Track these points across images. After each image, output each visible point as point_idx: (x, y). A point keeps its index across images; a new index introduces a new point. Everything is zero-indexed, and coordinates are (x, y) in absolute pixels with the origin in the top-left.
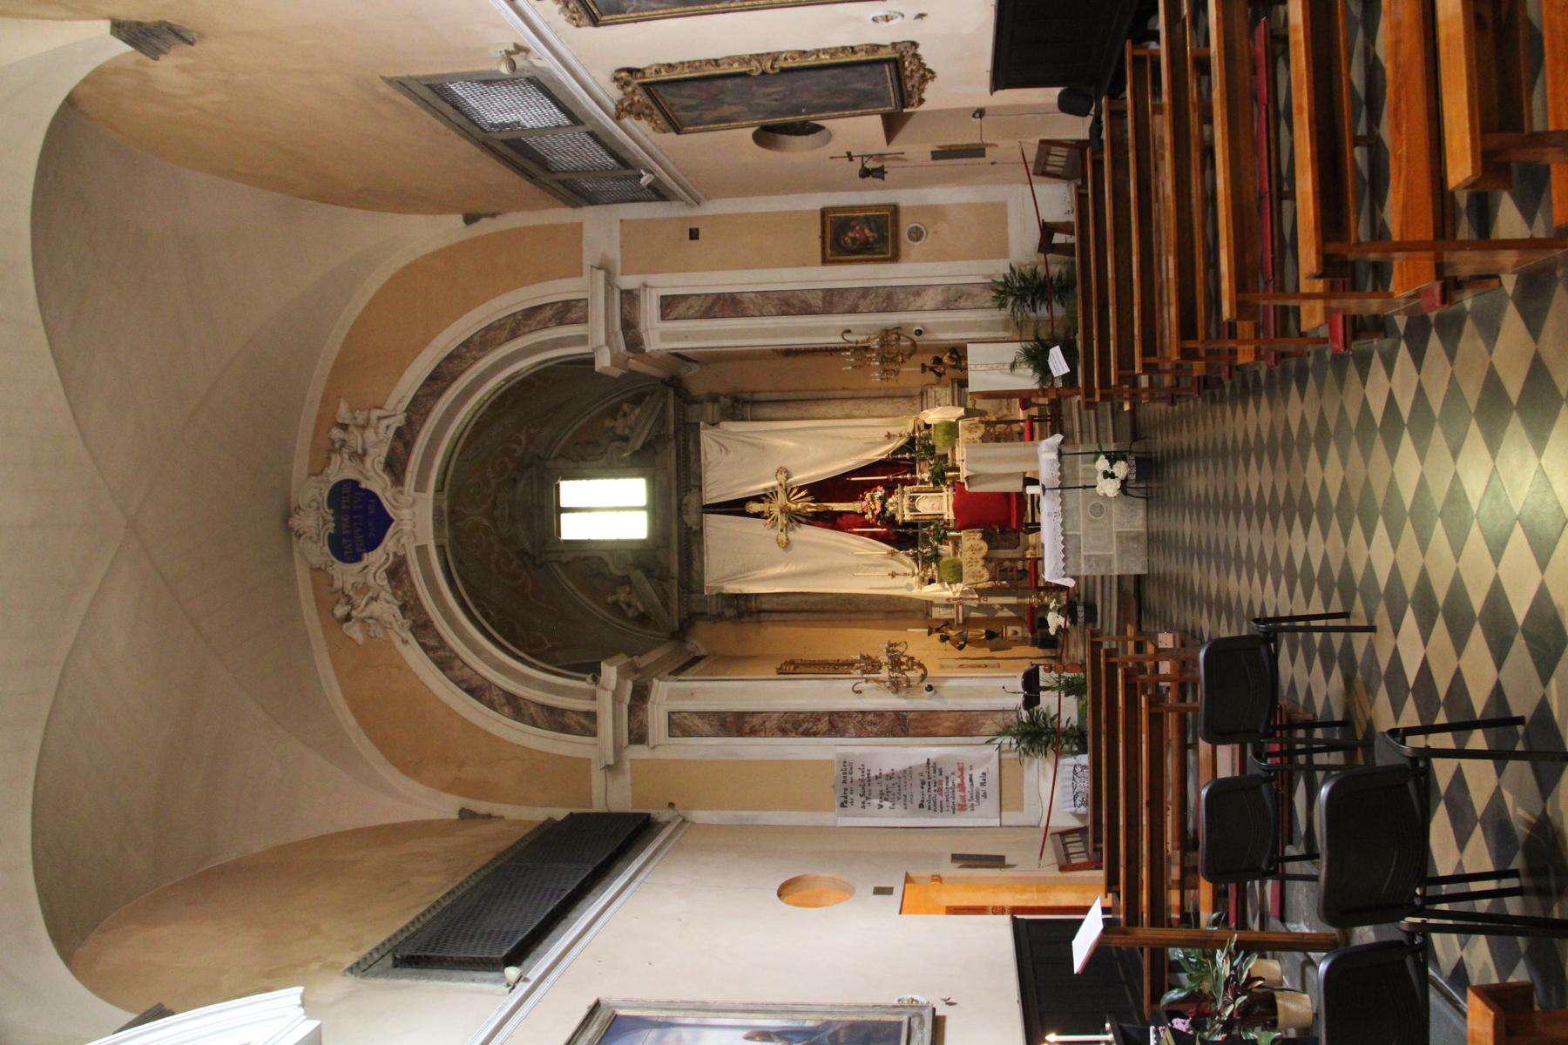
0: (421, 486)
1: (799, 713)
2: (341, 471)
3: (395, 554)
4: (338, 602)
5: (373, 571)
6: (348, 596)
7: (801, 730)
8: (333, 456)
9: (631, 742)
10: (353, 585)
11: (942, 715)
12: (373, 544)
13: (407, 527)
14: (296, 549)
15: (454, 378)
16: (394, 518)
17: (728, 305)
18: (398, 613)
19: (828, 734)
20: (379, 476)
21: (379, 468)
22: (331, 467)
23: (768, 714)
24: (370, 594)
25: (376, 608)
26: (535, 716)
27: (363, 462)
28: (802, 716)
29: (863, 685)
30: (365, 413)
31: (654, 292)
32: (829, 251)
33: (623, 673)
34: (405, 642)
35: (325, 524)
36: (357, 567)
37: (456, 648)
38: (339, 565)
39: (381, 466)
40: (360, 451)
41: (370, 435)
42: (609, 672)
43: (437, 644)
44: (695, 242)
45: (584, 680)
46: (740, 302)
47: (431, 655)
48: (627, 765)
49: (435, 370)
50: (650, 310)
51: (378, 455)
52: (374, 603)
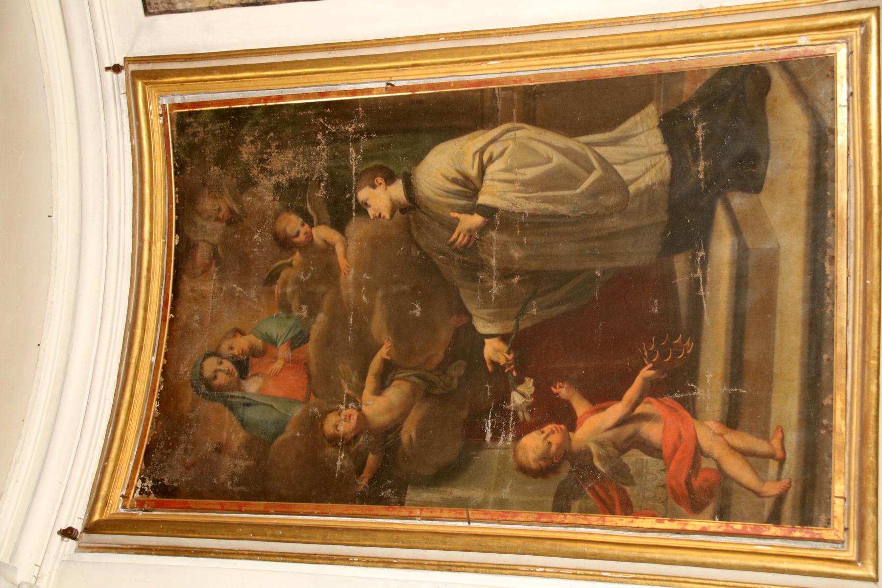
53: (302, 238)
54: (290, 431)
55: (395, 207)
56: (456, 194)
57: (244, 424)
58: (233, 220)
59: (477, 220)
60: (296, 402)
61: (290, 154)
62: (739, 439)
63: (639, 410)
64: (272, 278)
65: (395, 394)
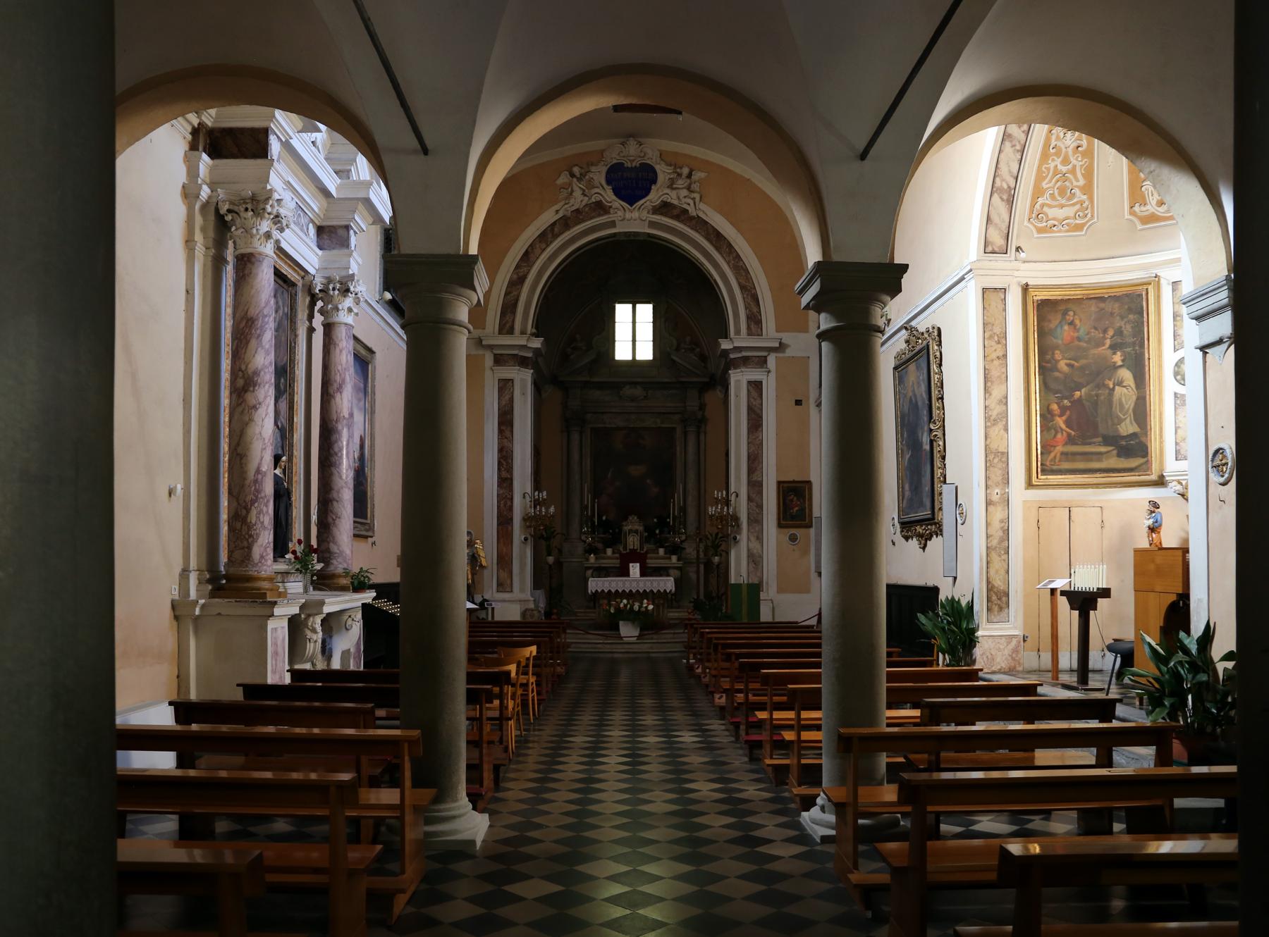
0: (652, 224)
1: (512, 460)
2: (663, 173)
3: (611, 207)
4: (581, 168)
5: (600, 192)
6: (586, 175)
7: (502, 460)
8: (673, 167)
9: (495, 355)
10: (592, 178)
11: (510, 546)
12: (617, 193)
13: (628, 215)
14: (615, 140)
15: (718, 249)
16: (634, 207)
17: (755, 422)
18: (574, 208)
19: (500, 477)
20: (660, 197)
21: (665, 198)
22: (665, 167)
23: (511, 441)
24: (587, 191)
25: (578, 193)
26: (512, 295)
27: (668, 187)
28: (510, 461)
29: (528, 499)
30: (698, 190)
31: (765, 377)
32: (786, 485)
33: (536, 351)
34: (557, 212)
35: (630, 161)
36: (604, 183)
37: (552, 246)
38: (604, 169)
39: (665, 200)
40: (674, 186)
41: (684, 192)
42: (537, 343)
43: (555, 233)
44: (794, 402)
45: (532, 327)
46: (757, 430)
47: (549, 229)
48: (481, 352)
49: (723, 236)
50: (755, 374)
51: (672, 198)
52: (581, 192)
53: (1107, 336)
54: (1055, 341)
55: (1115, 363)
56: (1118, 380)
57: (1057, 327)
58: (1112, 314)
59: (1111, 386)
60: (1062, 340)
61: (1130, 330)
62: (1058, 455)
63: (1064, 432)
64: (1096, 329)
65: (1066, 369)
